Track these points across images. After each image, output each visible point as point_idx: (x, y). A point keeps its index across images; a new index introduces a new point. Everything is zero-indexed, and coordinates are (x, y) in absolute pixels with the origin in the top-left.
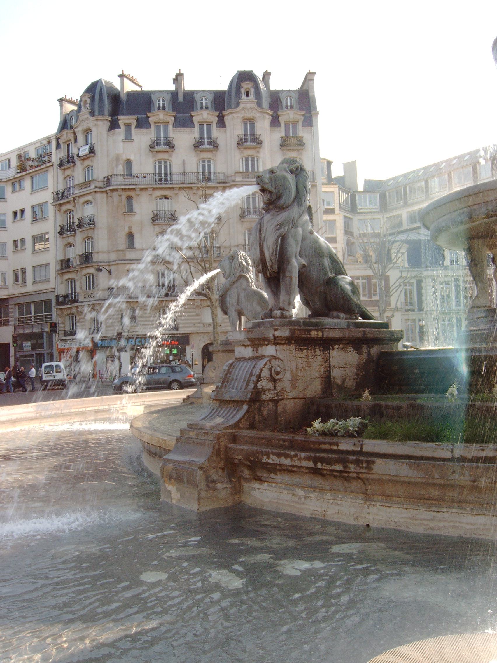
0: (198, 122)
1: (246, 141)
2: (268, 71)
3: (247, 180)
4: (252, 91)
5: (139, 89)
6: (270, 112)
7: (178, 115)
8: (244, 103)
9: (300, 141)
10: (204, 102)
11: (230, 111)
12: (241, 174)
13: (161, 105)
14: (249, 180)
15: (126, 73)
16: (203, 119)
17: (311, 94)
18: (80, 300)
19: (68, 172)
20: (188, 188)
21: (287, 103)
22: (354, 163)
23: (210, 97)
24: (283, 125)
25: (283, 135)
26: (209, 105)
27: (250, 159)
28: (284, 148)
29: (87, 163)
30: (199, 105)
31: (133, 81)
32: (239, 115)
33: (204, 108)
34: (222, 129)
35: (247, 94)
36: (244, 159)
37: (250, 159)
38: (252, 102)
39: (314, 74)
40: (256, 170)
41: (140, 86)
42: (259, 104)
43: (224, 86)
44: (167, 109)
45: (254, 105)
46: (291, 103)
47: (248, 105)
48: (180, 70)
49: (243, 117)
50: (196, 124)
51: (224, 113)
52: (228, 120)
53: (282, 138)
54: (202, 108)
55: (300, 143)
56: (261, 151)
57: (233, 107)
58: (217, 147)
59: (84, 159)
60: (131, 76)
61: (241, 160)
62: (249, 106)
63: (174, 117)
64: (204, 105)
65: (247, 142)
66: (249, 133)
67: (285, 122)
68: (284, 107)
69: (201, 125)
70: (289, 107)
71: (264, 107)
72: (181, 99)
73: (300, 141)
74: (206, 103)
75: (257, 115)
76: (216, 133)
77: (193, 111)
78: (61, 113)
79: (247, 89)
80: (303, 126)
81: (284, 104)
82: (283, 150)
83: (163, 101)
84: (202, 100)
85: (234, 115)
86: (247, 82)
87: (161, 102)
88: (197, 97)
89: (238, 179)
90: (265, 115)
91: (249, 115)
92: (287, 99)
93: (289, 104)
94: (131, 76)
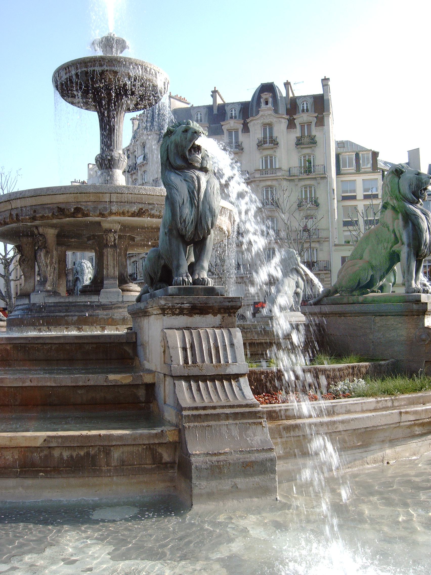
0: (227, 130)
1: (265, 142)
2: (289, 81)
3: (267, 176)
4: (270, 100)
5: (189, 106)
6: (288, 117)
7: (211, 126)
8: (263, 111)
9: (312, 139)
10: (233, 112)
11: (251, 118)
12: (259, 171)
13: (199, 118)
14: (268, 176)
15: (173, 95)
16: (231, 127)
17: (325, 98)
18: (138, 279)
19: (134, 177)
20: (275, 179)
21: (303, 107)
22: (417, 150)
23: (238, 108)
24: (298, 127)
25: (299, 134)
26: (237, 115)
27: (269, 158)
28: (299, 146)
29: (143, 169)
30: (229, 115)
31: (180, 100)
32: (259, 121)
33: (234, 117)
34: (246, 134)
35: (267, 103)
36: (264, 158)
37: (269, 158)
38: (269, 109)
39: (328, 79)
40: (274, 167)
41: (188, 104)
42: (276, 111)
43: (248, 98)
44: (203, 121)
45: (271, 112)
46: (307, 107)
47: (266, 112)
48: (215, 88)
49: (262, 123)
50: (225, 131)
51: (248, 121)
52: (250, 125)
53: (297, 138)
54: (231, 118)
55: (313, 142)
56: (278, 151)
57: (254, 115)
58: (242, 149)
59: (143, 165)
60: (179, 96)
61: (261, 160)
62: (266, 113)
63: (208, 128)
64: (233, 115)
65: (266, 143)
66: (268, 136)
67: (300, 124)
68: (300, 111)
69: (230, 132)
70: (305, 111)
71: (280, 112)
72: (215, 112)
73: (312, 139)
74: (235, 113)
75: (273, 120)
76: (242, 138)
77: (224, 120)
78: (133, 129)
79: (266, 99)
80: (316, 126)
81: (301, 108)
82: (298, 148)
83: (201, 114)
84: (232, 111)
85: (254, 121)
86: (265, 93)
87: (199, 116)
88: (227, 109)
89: (257, 175)
90: (280, 119)
91: (267, 121)
92: (303, 104)
93: (305, 108)
94: (179, 96)
